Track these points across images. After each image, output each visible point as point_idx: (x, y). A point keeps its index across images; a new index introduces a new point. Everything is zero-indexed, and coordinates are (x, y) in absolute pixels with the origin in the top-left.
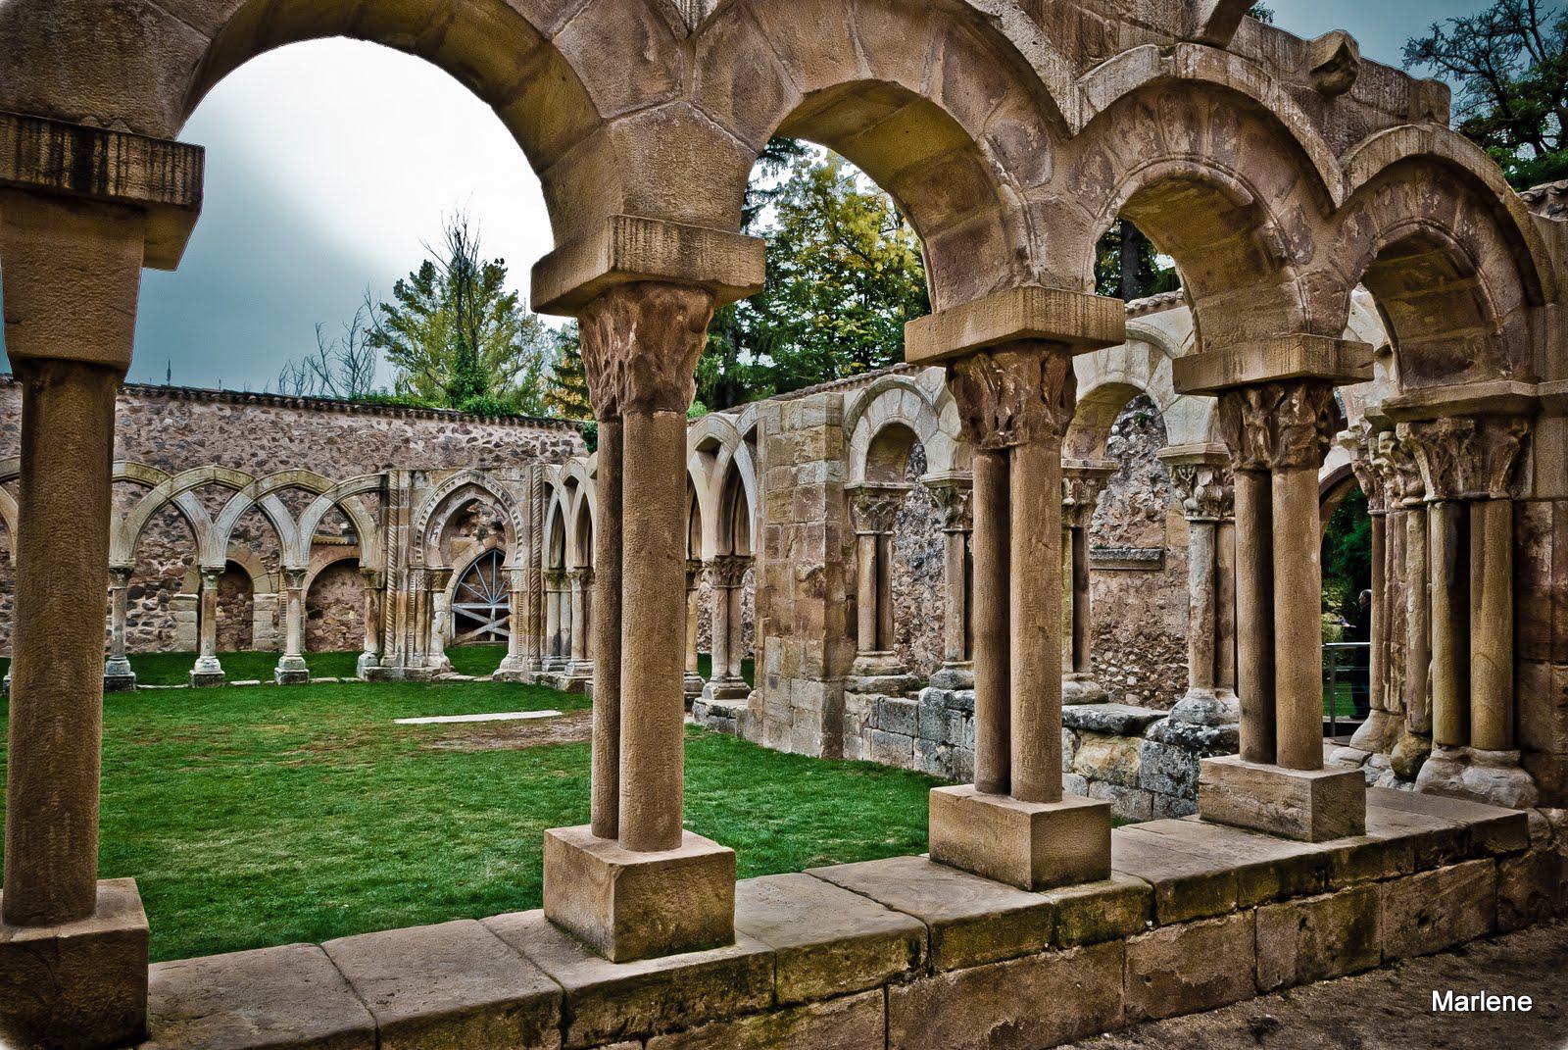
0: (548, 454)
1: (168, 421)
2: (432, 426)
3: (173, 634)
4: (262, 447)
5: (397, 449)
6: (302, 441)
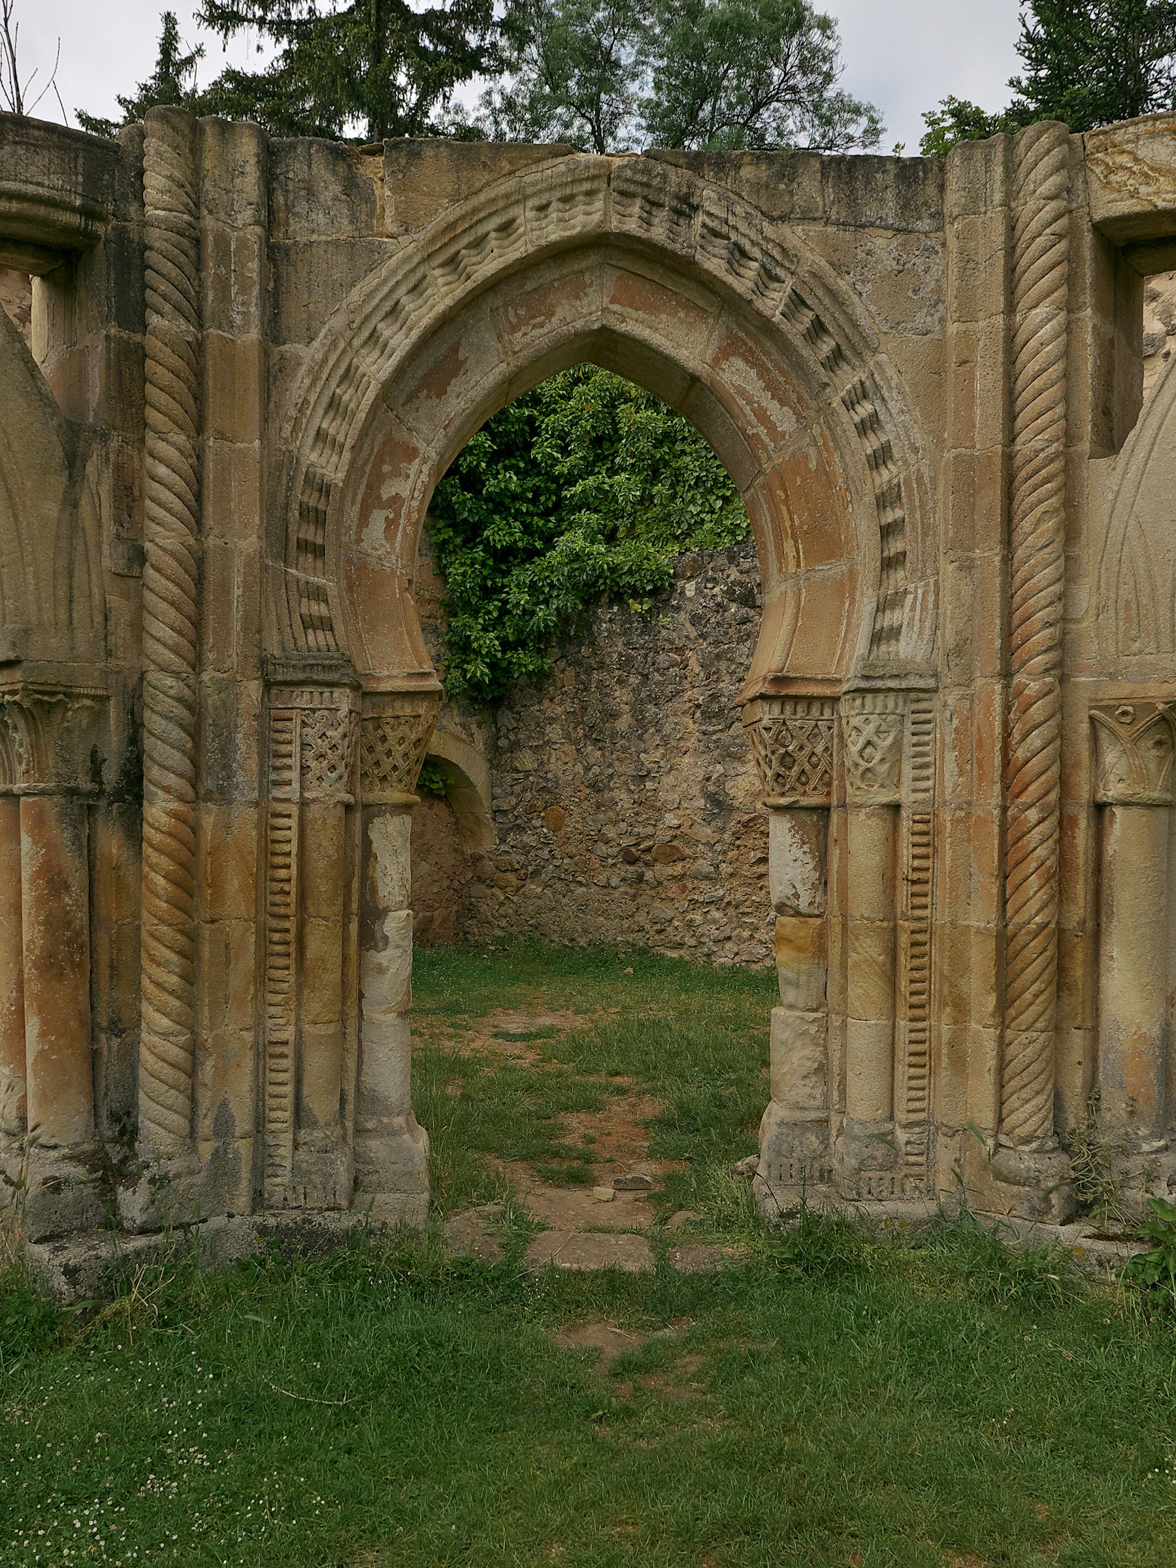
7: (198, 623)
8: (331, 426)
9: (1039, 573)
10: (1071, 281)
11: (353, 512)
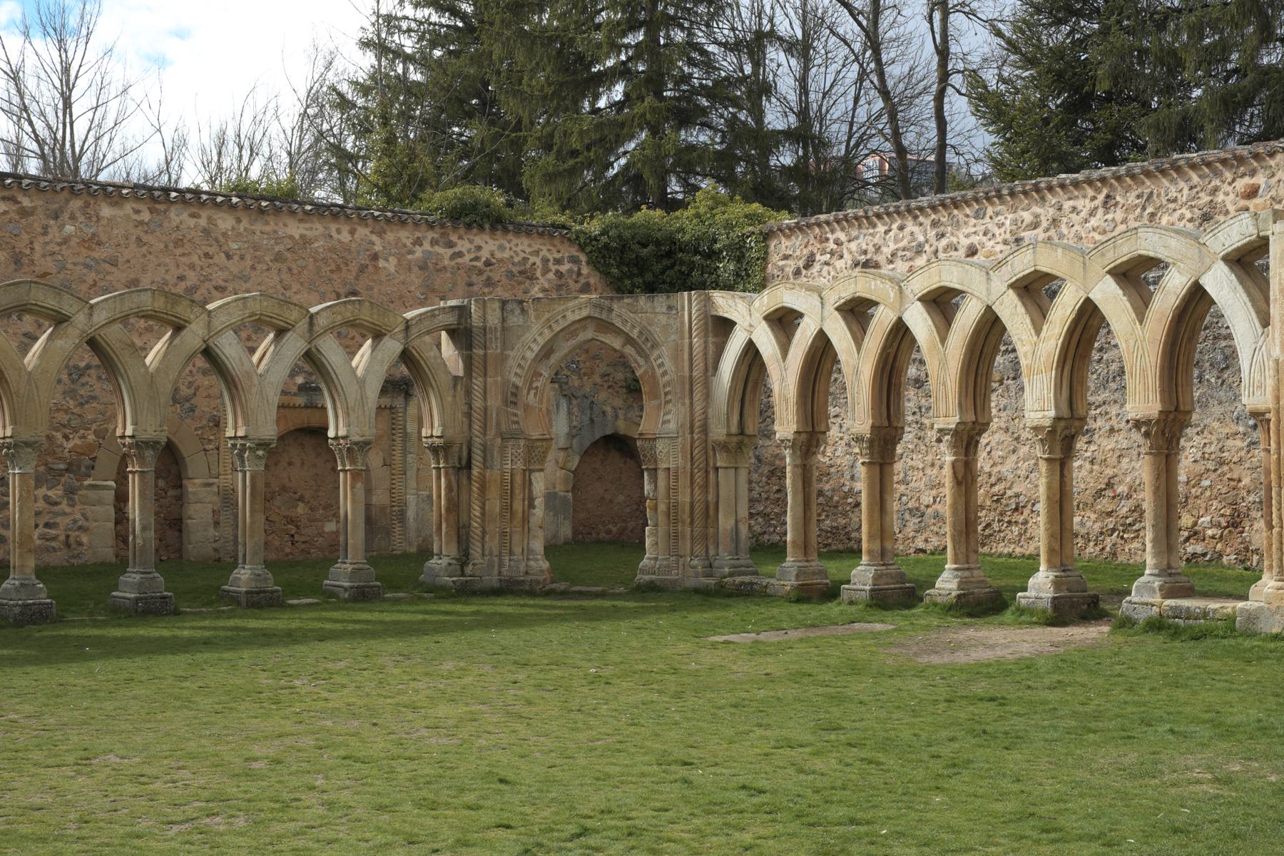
0: (551, 275)
1: (69, 229)
2: (405, 236)
3: (85, 539)
4: (192, 267)
5: (362, 269)
6: (242, 257)
7: (485, 425)
8: (519, 371)
9: (698, 408)
10: (706, 329)
11: (525, 391)
